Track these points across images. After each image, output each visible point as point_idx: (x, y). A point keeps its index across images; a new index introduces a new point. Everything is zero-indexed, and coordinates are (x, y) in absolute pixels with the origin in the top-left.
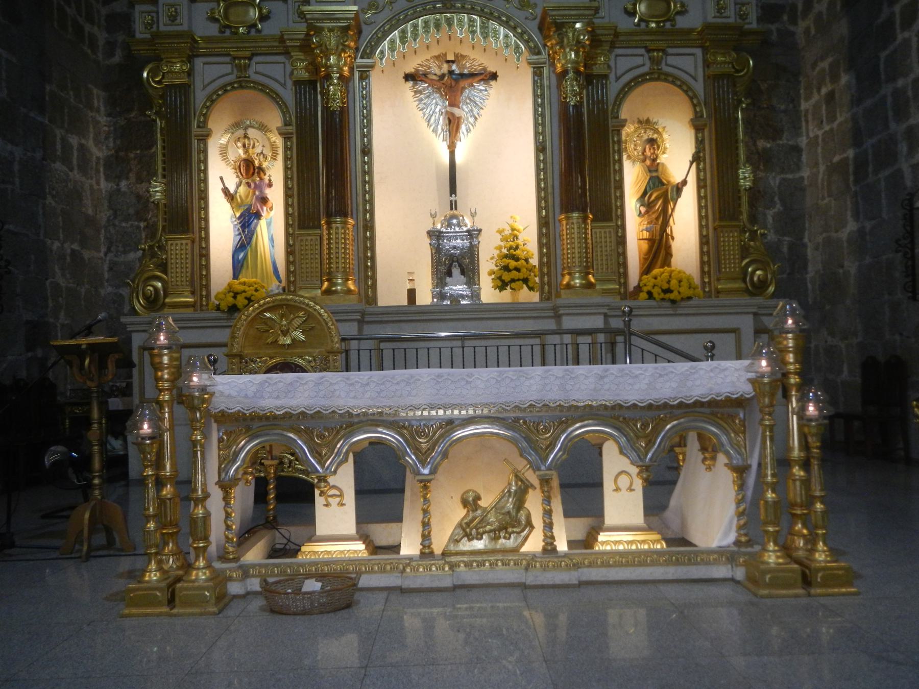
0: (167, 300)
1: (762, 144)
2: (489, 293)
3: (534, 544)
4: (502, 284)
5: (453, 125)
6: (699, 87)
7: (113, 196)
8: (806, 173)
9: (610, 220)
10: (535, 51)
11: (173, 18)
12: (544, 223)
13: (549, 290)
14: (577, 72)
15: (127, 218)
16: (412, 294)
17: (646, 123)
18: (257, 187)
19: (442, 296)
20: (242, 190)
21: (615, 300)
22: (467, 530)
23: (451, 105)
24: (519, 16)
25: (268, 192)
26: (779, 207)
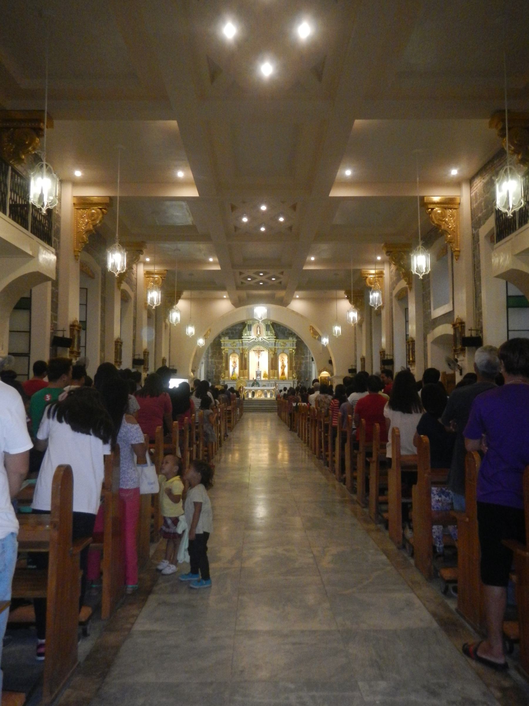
0: (226, 378)
1: (303, 356)
2: (262, 379)
3: (262, 397)
4: (264, 377)
5: (259, 357)
6: (288, 354)
7: (211, 362)
8: (308, 361)
9: (276, 370)
10: (268, 350)
11: (227, 345)
12: (269, 370)
13: (269, 378)
14: (273, 354)
15: (213, 365)
16: (253, 378)
17: (282, 358)
18: (236, 365)
19: (257, 378)
20: (233, 365)
21: (277, 379)
22: (258, 396)
23: (259, 355)
24: (267, 346)
25: (237, 365)
26: (304, 365)
